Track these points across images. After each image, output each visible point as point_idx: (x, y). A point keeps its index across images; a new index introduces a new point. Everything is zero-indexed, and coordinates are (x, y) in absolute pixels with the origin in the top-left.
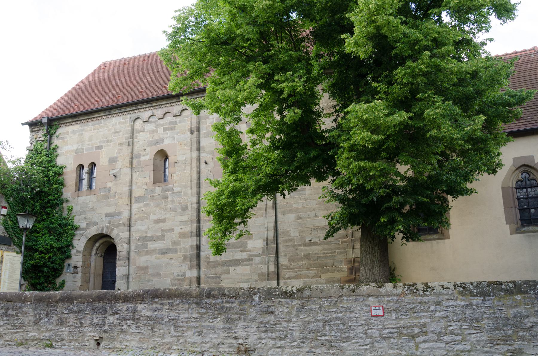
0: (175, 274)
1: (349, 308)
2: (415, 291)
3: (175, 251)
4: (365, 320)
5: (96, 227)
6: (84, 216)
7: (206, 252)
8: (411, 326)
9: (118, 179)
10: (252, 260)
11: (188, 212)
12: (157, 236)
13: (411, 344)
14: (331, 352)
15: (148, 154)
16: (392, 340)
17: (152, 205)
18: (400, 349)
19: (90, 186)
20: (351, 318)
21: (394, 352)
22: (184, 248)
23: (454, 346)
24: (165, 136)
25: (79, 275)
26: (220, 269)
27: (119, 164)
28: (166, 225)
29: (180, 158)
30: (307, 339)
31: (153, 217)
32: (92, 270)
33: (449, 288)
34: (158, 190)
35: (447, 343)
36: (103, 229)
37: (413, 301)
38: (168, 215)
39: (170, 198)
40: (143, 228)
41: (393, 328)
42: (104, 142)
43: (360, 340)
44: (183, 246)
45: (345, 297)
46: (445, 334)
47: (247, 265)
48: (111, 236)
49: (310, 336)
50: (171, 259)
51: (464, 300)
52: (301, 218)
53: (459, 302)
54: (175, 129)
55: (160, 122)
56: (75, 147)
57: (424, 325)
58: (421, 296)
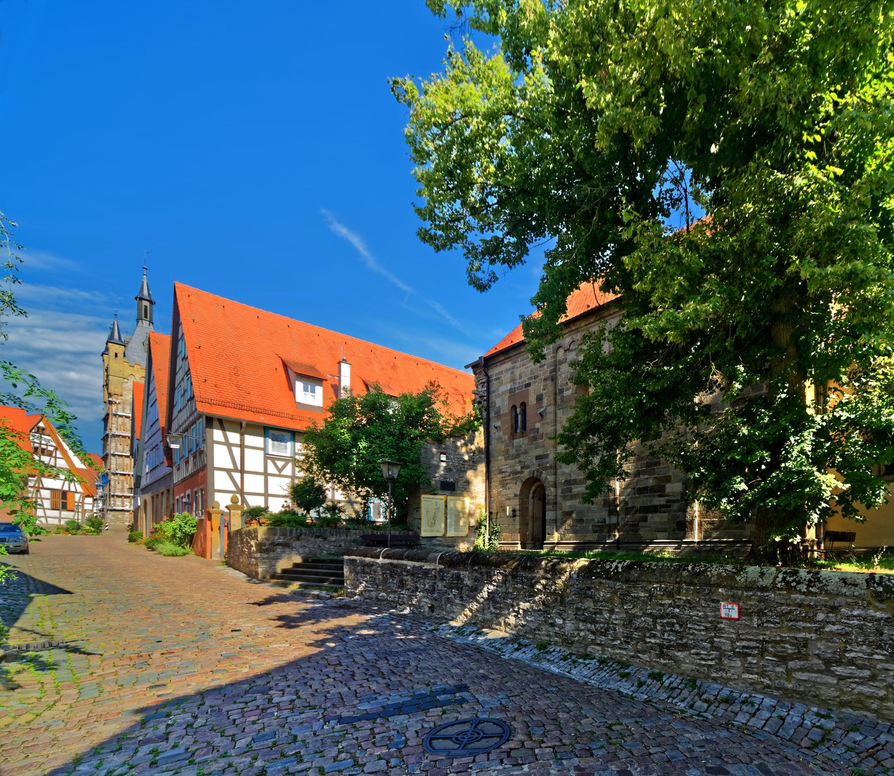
1: (689, 602)
2: (793, 584)
4: (711, 622)
8: (782, 641)
13: (778, 669)
14: (662, 661)
16: (749, 659)
18: (762, 674)
19: (524, 427)
20: (691, 616)
21: (751, 676)
23: (854, 686)
25: (517, 518)
27: (545, 402)
30: (632, 639)
32: (530, 514)
33: (856, 585)
35: (841, 678)
37: (789, 602)
41: (751, 640)
42: (531, 378)
43: (702, 652)
45: (684, 586)
46: (839, 663)
49: (636, 635)
51: (882, 610)
53: (871, 612)
57: (806, 643)
58: (804, 593)
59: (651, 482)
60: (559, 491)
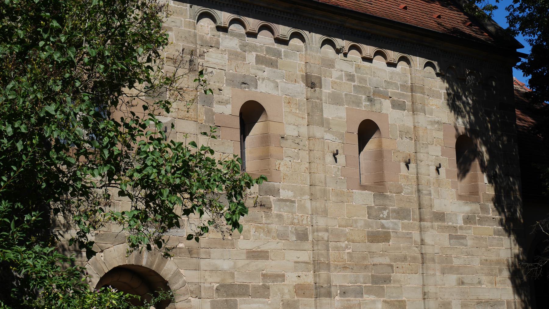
11: (308, 245)
15: (226, 103)
28: (271, 266)
29: (290, 131)
38: (272, 245)
39: (275, 211)
40: (226, 265)
48: (162, 273)
52: (463, 283)
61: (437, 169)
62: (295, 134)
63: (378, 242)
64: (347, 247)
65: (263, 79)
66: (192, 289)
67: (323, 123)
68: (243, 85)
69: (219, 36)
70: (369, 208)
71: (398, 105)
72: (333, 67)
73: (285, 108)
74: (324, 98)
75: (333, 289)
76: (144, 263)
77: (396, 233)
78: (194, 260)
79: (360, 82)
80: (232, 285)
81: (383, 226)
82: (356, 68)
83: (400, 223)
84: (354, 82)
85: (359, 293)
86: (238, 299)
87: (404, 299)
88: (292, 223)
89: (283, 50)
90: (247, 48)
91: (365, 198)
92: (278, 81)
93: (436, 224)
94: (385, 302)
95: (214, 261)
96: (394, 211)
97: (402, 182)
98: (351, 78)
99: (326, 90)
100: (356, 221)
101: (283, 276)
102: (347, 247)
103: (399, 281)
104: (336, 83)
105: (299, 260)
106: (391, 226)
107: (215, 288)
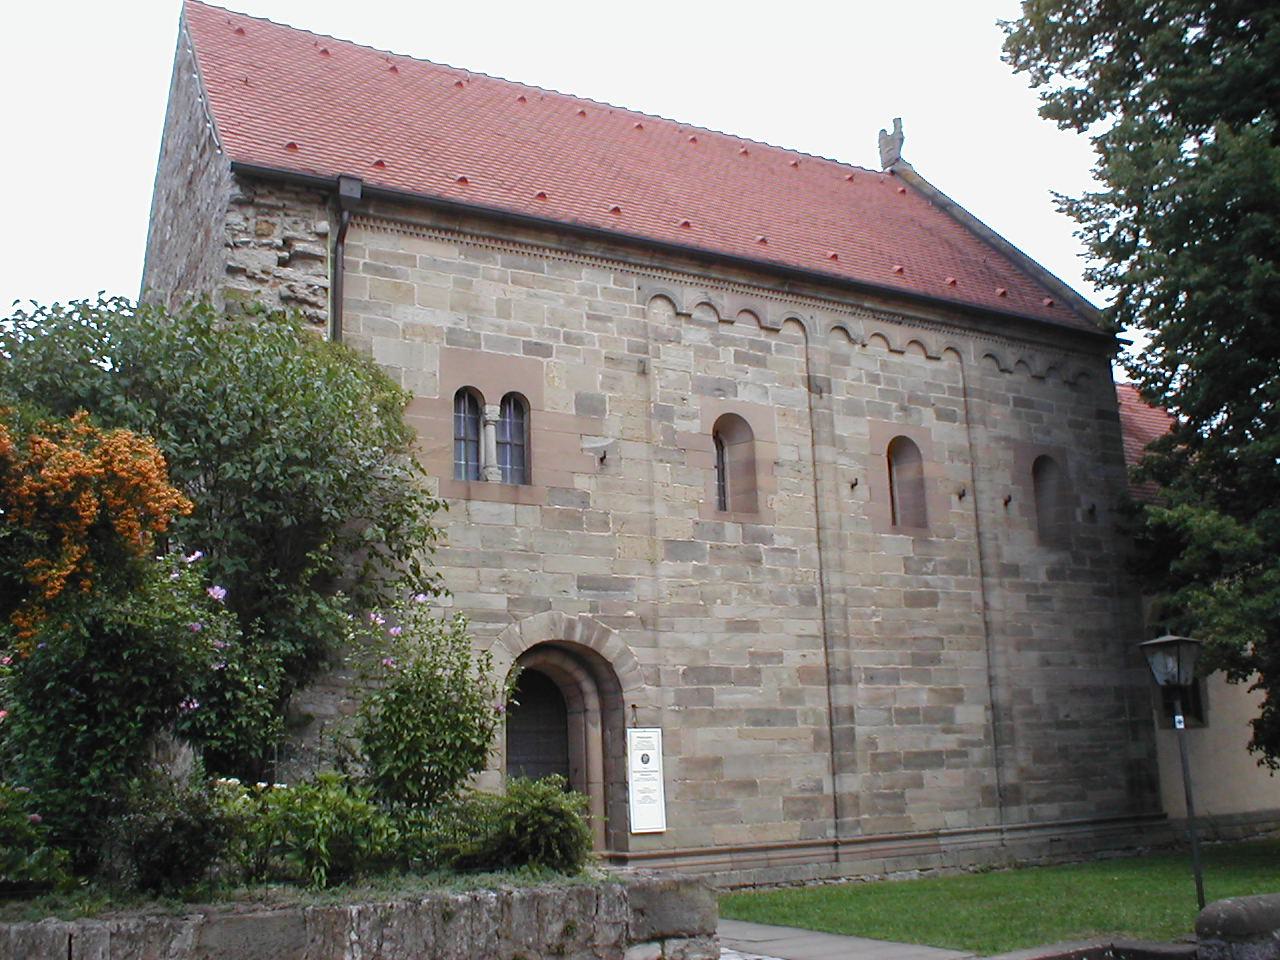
0: (795, 786)
3: (791, 719)
5: (545, 614)
6: (497, 572)
7: (866, 729)
9: (612, 469)
10: (965, 754)
12: (738, 671)
15: (694, 416)
17: (718, 573)
22: (814, 711)
24: (741, 376)
26: (903, 773)
27: (613, 423)
28: (762, 641)
29: (787, 454)
31: (722, 612)
34: (732, 532)
36: (571, 625)
38: (762, 612)
39: (766, 565)
40: (696, 640)
42: (556, 335)
44: (809, 705)
47: (957, 767)
48: (603, 652)
50: (783, 741)
54: (765, 366)
55: (724, 330)
56: (444, 320)
59: (924, 699)
60: (670, 697)
61: (1006, 503)
62: (795, 457)
63: (921, 606)
64: (874, 614)
65: (746, 384)
66: (646, 673)
67: (835, 441)
68: (717, 393)
69: (680, 326)
70: (906, 559)
71: (943, 415)
72: (848, 365)
73: (778, 423)
74: (835, 408)
75: (854, 673)
76: (577, 637)
77: (948, 593)
78: (649, 634)
79: (887, 384)
80: (705, 669)
81: (927, 585)
82: (881, 365)
83: (952, 579)
84: (879, 384)
85: (894, 677)
86: (714, 687)
87: (961, 686)
88: (793, 582)
89: (774, 343)
90: (721, 342)
91: (899, 545)
92: (767, 385)
93: (1007, 581)
94: (931, 690)
95: (677, 635)
96: (943, 563)
97: (954, 523)
98: (874, 379)
99: (839, 397)
100: (887, 578)
101: (781, 655)
102: (874, 614)
103: (953, 662)
104: (852, 386)
105: (803, 633)
106: (940, 583)
107: (681, 671)
